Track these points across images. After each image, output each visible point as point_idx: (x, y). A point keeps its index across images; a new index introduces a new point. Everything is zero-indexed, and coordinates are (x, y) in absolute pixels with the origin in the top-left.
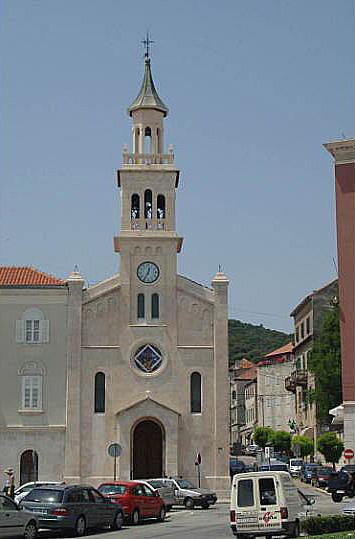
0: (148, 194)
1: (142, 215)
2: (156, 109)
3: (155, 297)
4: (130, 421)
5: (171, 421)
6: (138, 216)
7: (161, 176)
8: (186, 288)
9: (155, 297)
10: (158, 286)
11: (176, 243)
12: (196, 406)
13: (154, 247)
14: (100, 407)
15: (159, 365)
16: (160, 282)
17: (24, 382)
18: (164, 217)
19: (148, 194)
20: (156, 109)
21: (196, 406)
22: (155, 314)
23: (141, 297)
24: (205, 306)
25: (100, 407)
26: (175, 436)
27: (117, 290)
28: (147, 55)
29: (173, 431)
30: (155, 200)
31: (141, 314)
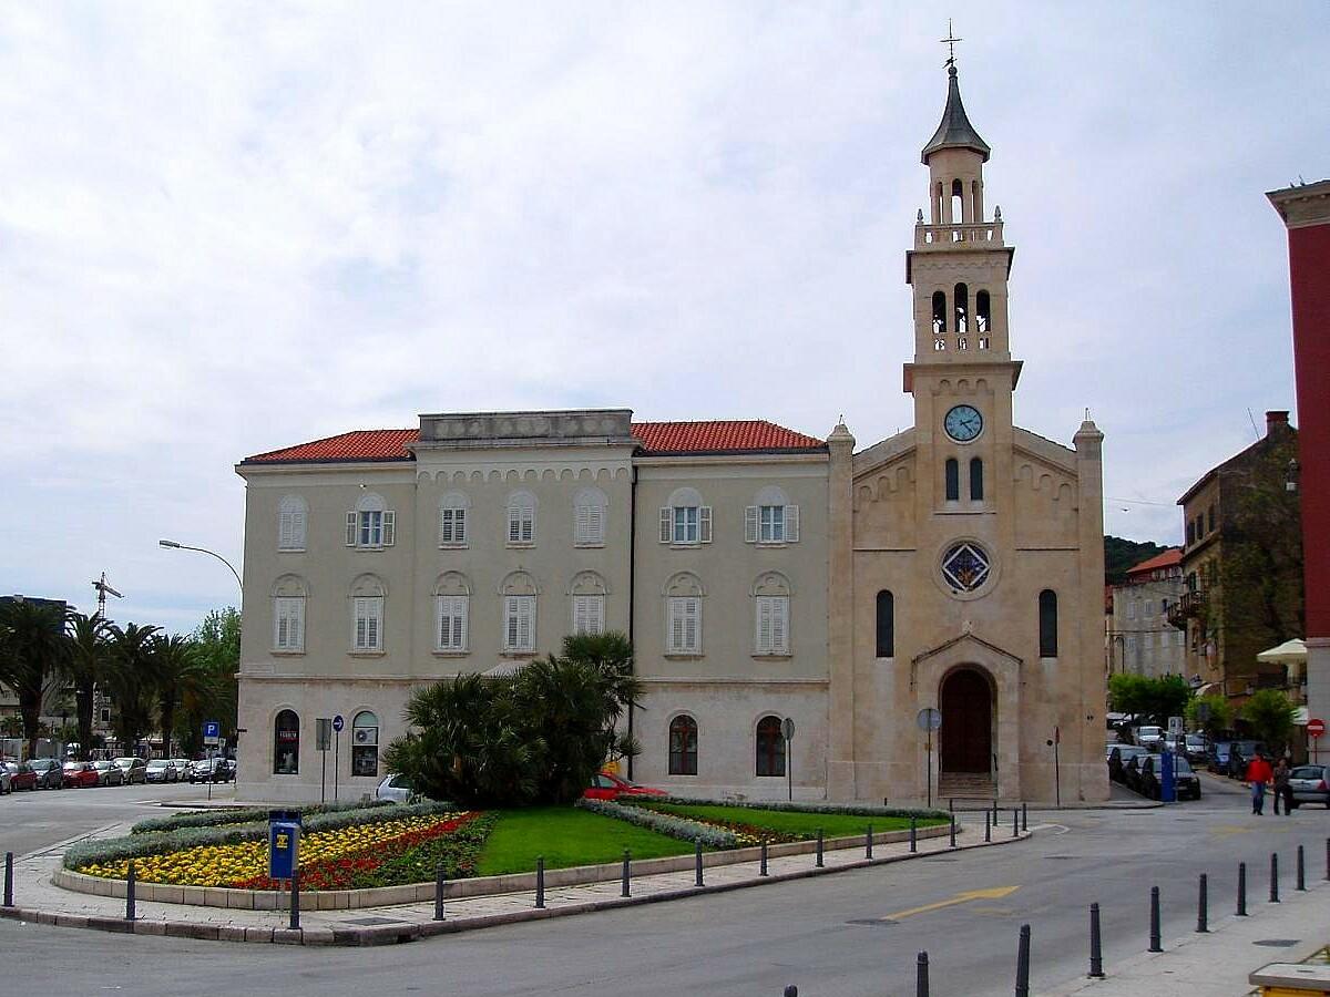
0: (961, 291)
1: (950, 327)
3: (976, 464)
4: (935, 670)
6: (943, 328)
7: (981, 260)
8: (1029, 450)
9: (976, 464)
10: (983, 445)
11: (1011, 371)
12: (1049, 647)
14: (885, 648)
15: (983, 578)
16: (984, 440)
17: (759, 607)
18: (988, 328)
19: (961, 291)
20: (970, 149)
21: (1049, 647)
22: (977, 494)
23: (952, 464)
24: (1061, 480)
25: (885, 648)
27: (911, 454)
28: (951, 61)
30: (972, 302)
31: (953, 494)
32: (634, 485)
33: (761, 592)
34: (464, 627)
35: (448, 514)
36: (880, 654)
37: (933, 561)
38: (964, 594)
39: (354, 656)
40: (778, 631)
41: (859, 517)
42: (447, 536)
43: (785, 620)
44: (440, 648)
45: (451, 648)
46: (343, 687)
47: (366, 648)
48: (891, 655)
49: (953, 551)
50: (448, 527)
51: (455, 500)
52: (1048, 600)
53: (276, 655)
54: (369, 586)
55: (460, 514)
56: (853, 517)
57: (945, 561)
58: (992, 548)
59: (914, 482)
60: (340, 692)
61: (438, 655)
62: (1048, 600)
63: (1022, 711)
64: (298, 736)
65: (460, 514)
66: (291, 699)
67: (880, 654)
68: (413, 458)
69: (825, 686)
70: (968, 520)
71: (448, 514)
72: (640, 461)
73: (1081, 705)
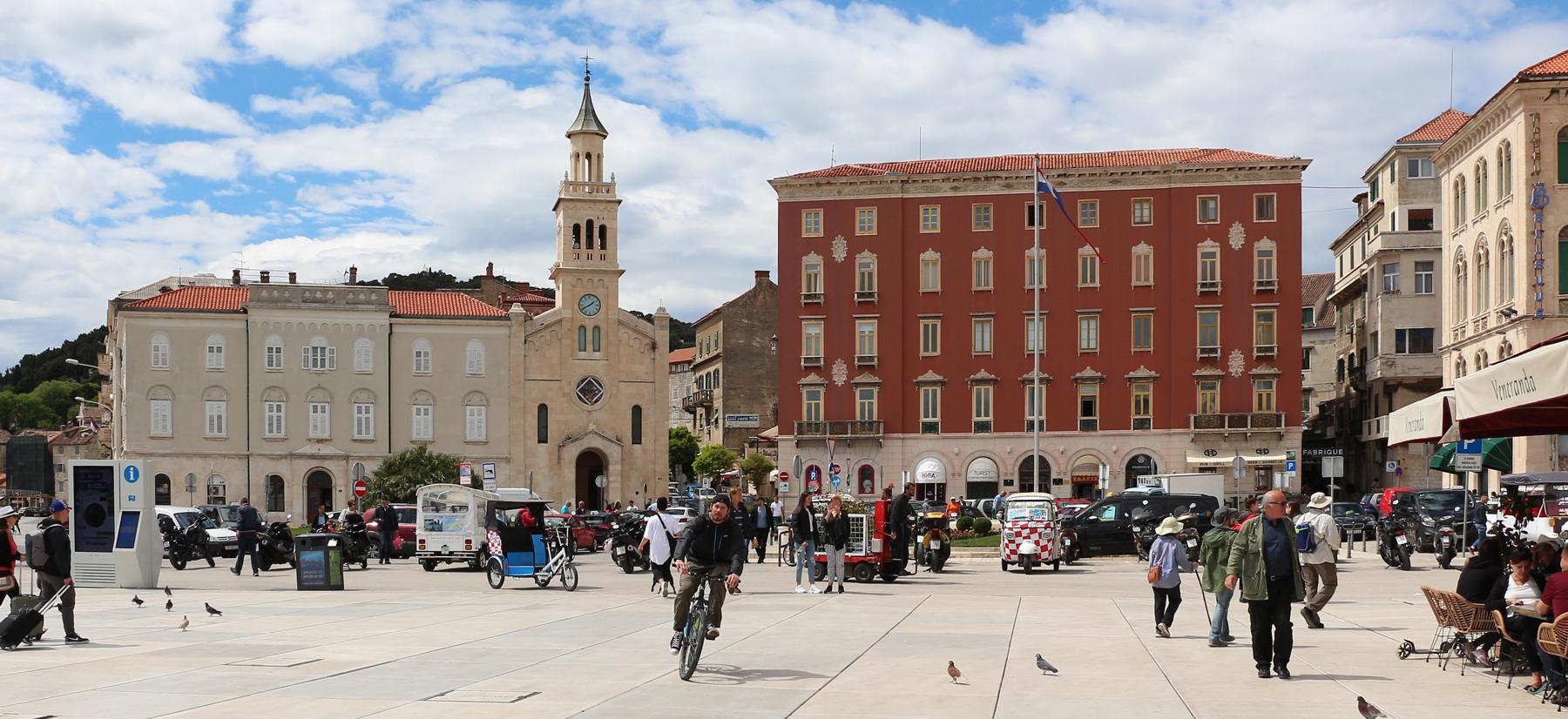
2: (597, 134)
4: (573, 452)
5: (615, 454)
12: (637, 439)
13: (596, 279)
14: (543, 439)
15: (600, 398)
17: (468, 413)
21: (637, 439)
25: (543, 439)
26: (619, 467)
29: (616, 462)
32: (390, 334)
33: (469, 403)
34: (283, 421)
35: (270, 349)
36: (539, 442)
37: (572, 389)
38: (589, 407)
39: (207, 439)
40: (479, 427)
41: (527, 358)
42: (270, 364)
43: (484, 421)
44: (268, 435)
45: (275, 434)
46: (200, 459)
47: (216, 434)
48: (547, 442)
49: (583, 381)
50: (270, 358)
51: (274, 341)
52: (637, 410)
53: (152, 438)
54: (216, 394)
55: (278, 350)
56: (525, 359)
57: (578, 387)
58: (605, 380)
59: (560, 340)
60: (199, 462)
61: (267, 440)
62: (637, 410)
63: (622, 474)
64: (169, 488)
65: (278, 350)
66: (165, 467)
67: (539, 442)
68: (245, 312)
69: (508, 460)
70: (593, 364)
71: (270, 349)
72: (394, 320)
73: (655, 471)
